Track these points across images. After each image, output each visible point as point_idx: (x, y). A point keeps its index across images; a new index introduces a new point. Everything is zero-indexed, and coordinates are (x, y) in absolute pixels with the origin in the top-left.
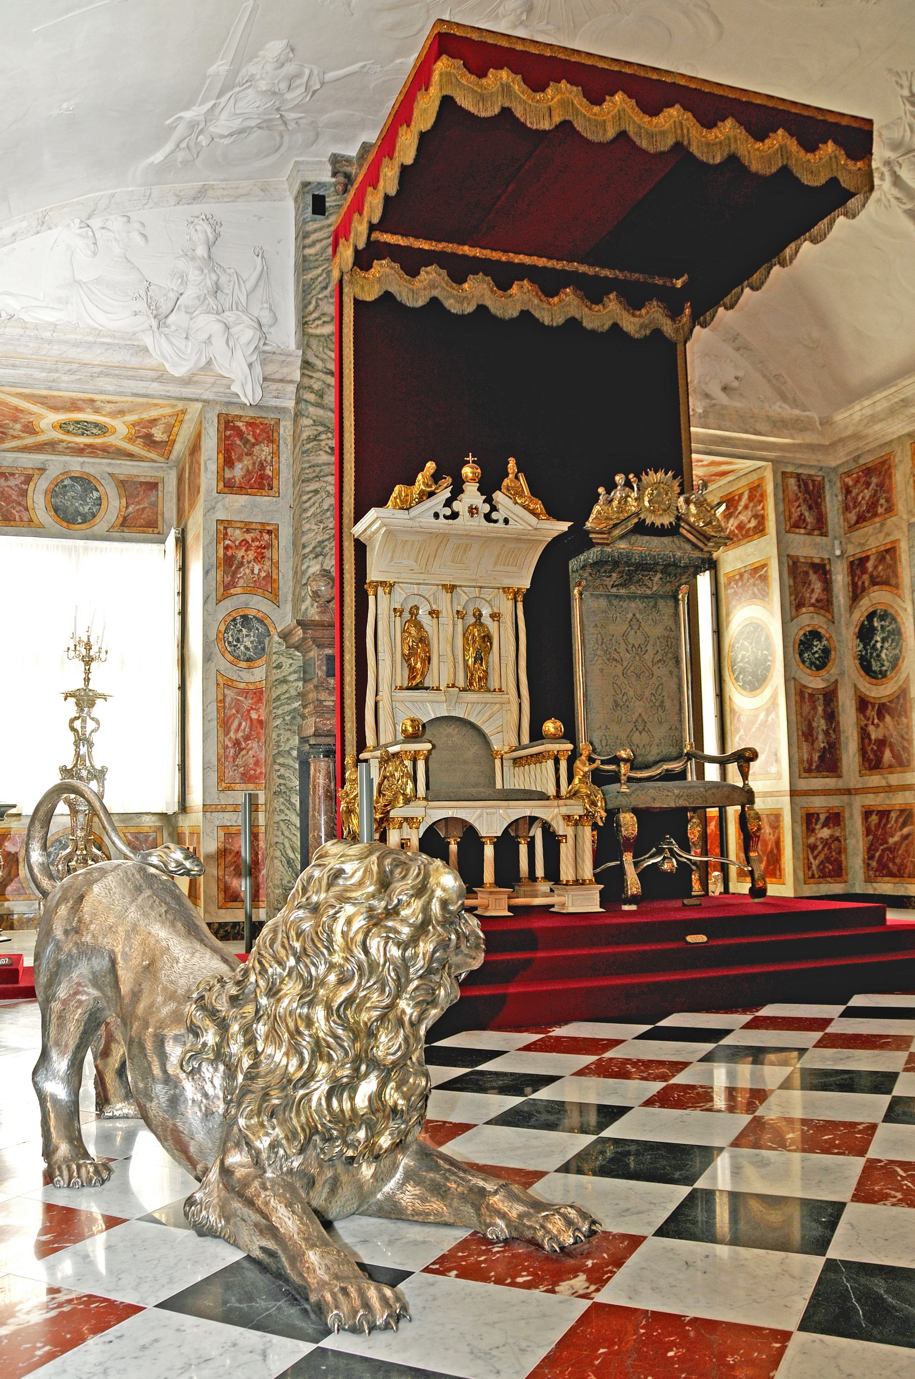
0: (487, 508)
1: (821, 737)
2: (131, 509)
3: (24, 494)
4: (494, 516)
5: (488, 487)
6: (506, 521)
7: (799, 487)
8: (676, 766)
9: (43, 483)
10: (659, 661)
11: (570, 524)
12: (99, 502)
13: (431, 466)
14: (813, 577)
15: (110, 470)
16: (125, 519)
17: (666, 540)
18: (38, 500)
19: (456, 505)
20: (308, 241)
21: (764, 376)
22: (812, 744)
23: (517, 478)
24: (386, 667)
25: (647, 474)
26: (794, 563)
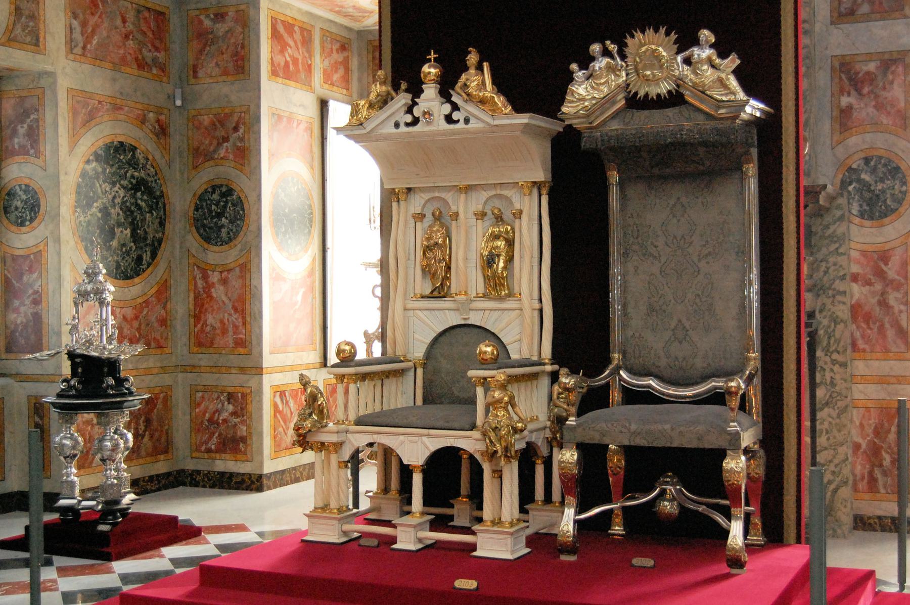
0: (447, 108)
6: (467, 121)
10: (710, 253)
17: (670, 112)
25: (633, 36)
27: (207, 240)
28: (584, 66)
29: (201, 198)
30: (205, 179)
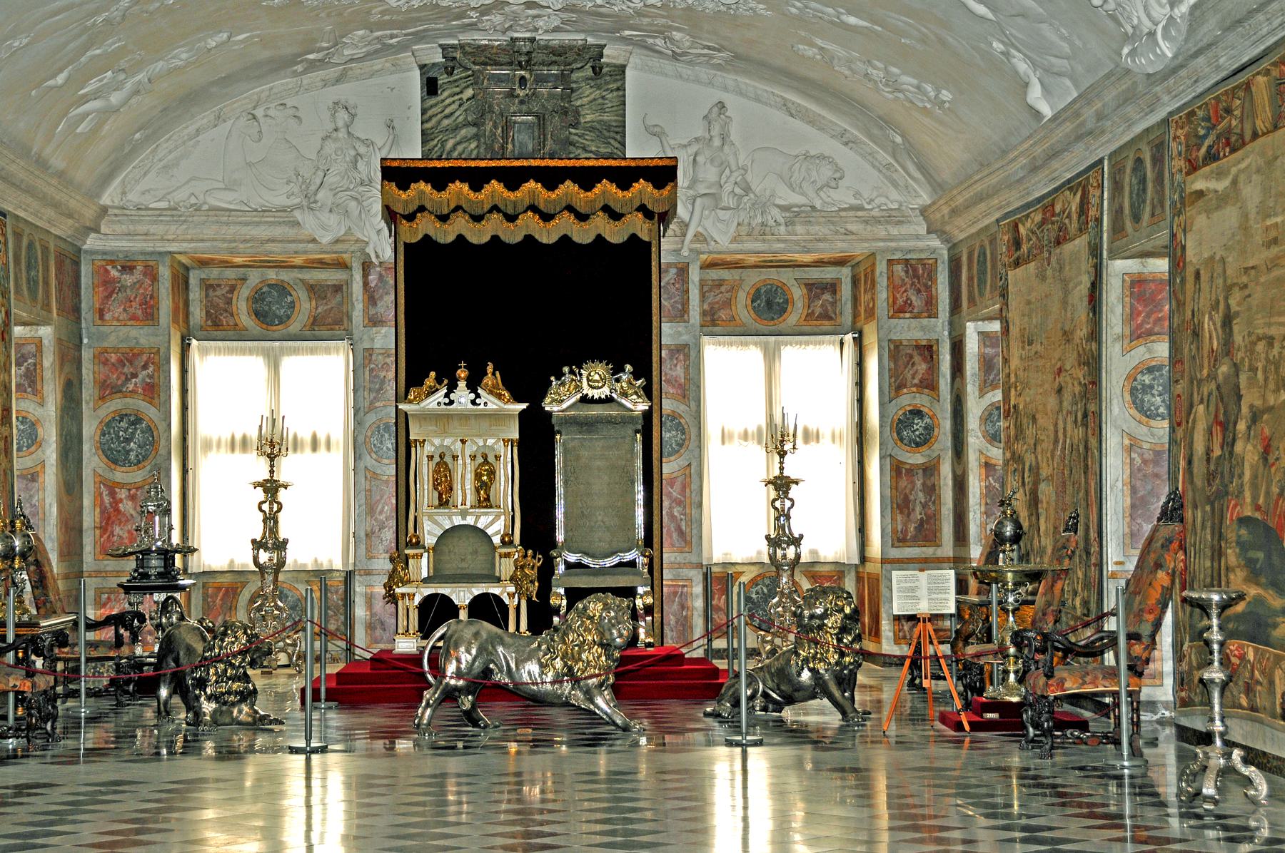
0: (472, 396)
1: (918, 509)
2: (320, 310)
3: (229, 302)
4: (478, 401)
5: (473, 386)
7: (907, 272)
8: (628, 557)
9: (245, 292)
11: (524, 406)
12: (292, 305)
13: (433, 374)
14: (917, 359)
15: (300, 276)
16: (315, 319)
18: (241, 306)
19: (452, 396)
20: (426, 117)
21: (874, 166)
22: (909, 514)
23: (494, 374)
24: (424, 492)
26: (897, 347)
27: (115, 462)
28: (558, 378)
29: (108, 425)
30: (112, 409)
